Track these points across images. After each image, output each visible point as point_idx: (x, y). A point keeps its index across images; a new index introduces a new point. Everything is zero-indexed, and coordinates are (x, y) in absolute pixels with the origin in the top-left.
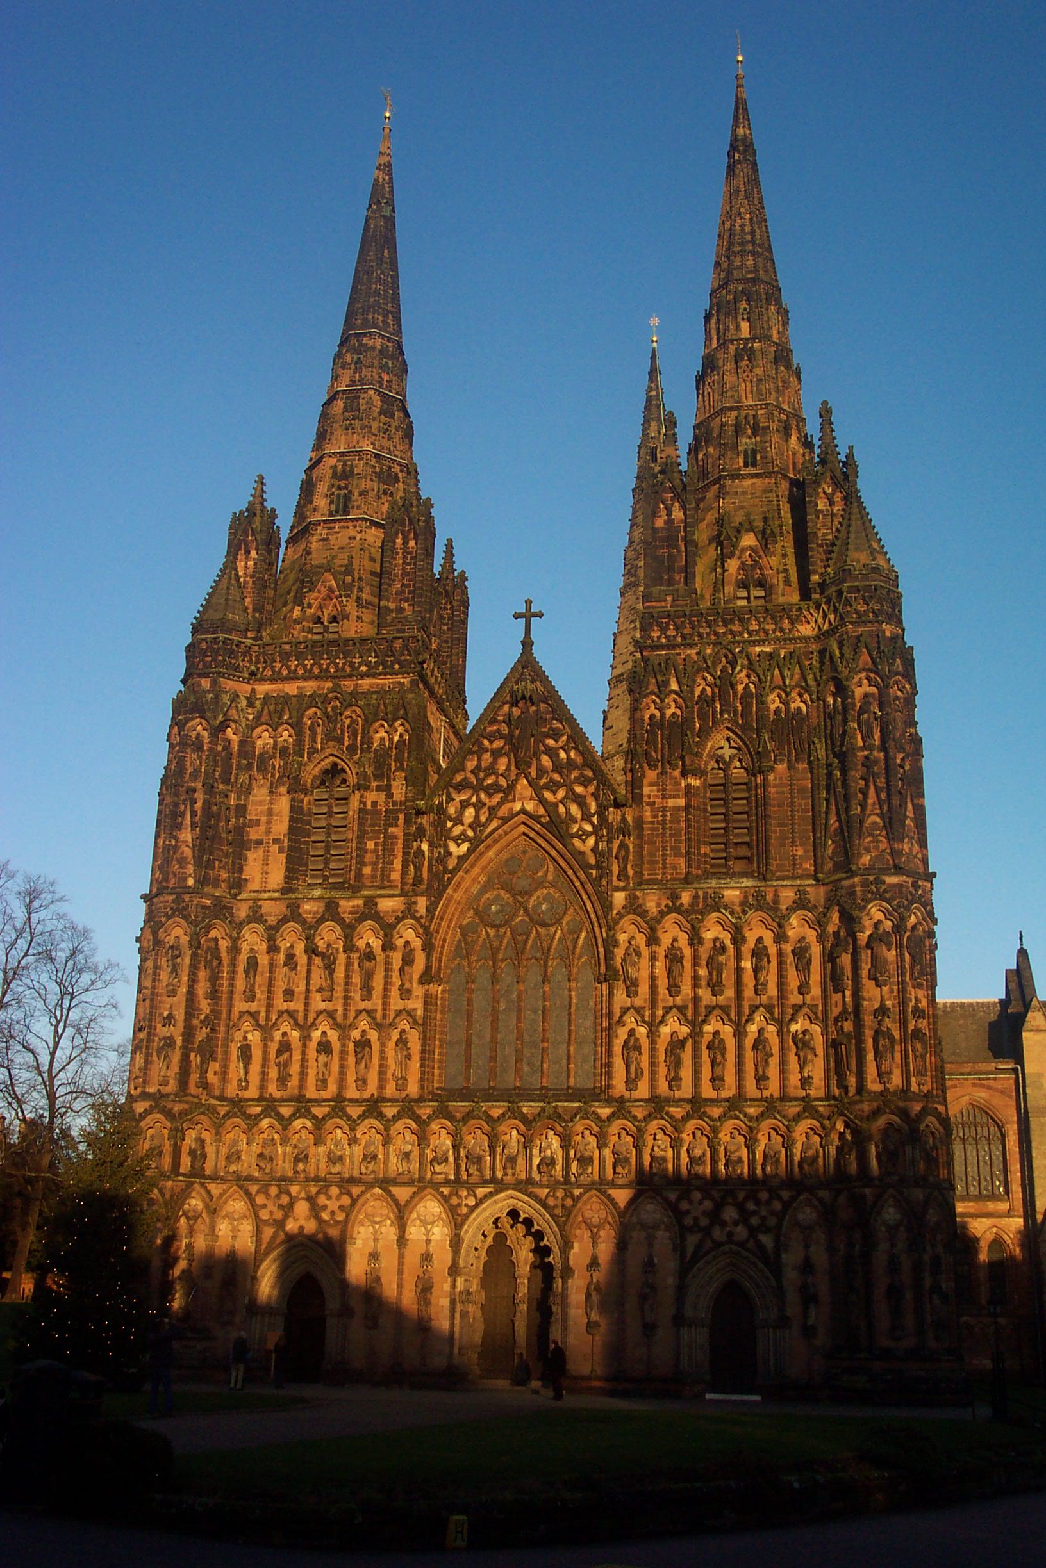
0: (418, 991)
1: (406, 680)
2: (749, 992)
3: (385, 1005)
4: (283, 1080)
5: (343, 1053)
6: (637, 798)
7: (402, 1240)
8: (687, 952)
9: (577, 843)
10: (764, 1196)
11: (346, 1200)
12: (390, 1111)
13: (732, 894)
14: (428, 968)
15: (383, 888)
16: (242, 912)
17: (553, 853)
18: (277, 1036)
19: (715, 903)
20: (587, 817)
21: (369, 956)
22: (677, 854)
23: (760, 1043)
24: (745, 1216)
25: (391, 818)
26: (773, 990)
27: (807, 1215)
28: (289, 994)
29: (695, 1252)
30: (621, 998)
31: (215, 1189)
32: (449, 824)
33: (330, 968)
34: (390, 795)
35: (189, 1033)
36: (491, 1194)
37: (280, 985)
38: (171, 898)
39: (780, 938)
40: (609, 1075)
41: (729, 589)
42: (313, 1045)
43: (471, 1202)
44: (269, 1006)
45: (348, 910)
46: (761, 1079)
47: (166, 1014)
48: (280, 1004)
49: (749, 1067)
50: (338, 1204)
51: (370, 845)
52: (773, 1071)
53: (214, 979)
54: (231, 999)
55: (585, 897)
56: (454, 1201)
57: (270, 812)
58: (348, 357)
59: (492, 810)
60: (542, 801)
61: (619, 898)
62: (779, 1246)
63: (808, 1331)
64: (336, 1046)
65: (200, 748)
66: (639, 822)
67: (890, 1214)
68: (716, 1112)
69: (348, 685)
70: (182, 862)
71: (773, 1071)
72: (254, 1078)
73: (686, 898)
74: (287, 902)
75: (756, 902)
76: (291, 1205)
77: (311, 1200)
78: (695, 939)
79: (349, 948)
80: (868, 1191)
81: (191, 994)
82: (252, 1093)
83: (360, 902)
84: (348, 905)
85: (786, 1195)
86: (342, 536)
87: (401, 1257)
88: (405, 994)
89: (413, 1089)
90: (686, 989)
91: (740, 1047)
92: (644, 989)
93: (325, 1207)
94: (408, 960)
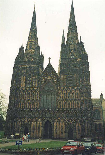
0: (39, 97)
1: (37, 65)
2: (72, 97)
3: (35, 99)
4: (25, 106)
5: (31, 103)
6: (60, 77)
7: (37, 123)
8: (66, 93)
9: (55, 82)
10: (74, 119)
11: (31, 119)
14: (40, 95)
15: (35, 86)
16: (20, 89)
18: (24, 102)
19: (69, 88)
20: (56, 79)
21: (34, 94)
23: (73, 103)
24: (72, 121)
25: (36, 79)
26: (74, 97)
27: (78, 121)
28: (25, 98)
30: (59, 98)
31: (17, 118)
33: (30, 95)
35: (15, 102)
36: (45, 119)
37: (24, 97)
39: (75, 92)
40: (58, 106)
41: (70, 56)
42: (28, 103)
43: (44, 119)
44: (23, 99)
46: (73, 107)
48: (24, 99)
49: (72, 105)
51: (34, 82)
52: (75, 106)
53: (17, 96)
54: (19, 98)
57: (23, 79)
58: (31, 31)
59: (46, 79)
60: (51, 78)
61: (59, 88)
62: (76, 124)
63: (79, 133)
64: (30, 103)
65: (16, 72)
66: (61, 80)
67: (87, 121)
68: (69, 110)
69: (31, 66)
70: (14, 84)
71: (75, 106)
72: (22, 107)
73: (65, 88)
75: (73, 88)
76: (25, 120)
77: (27, 119)
79: (32, 93)
80: (84, 118)
81: (15, 97)
82: (21, 108)
84: (31, 88)
85: (76, 119)
86: (30, 51)
87: (37, 125)
88: (37, 98)
89: (38, 107)
90: (66, 97)
91: (71, 103)
92: (61, 97)
93: (29, 120)
94: (38, 94)
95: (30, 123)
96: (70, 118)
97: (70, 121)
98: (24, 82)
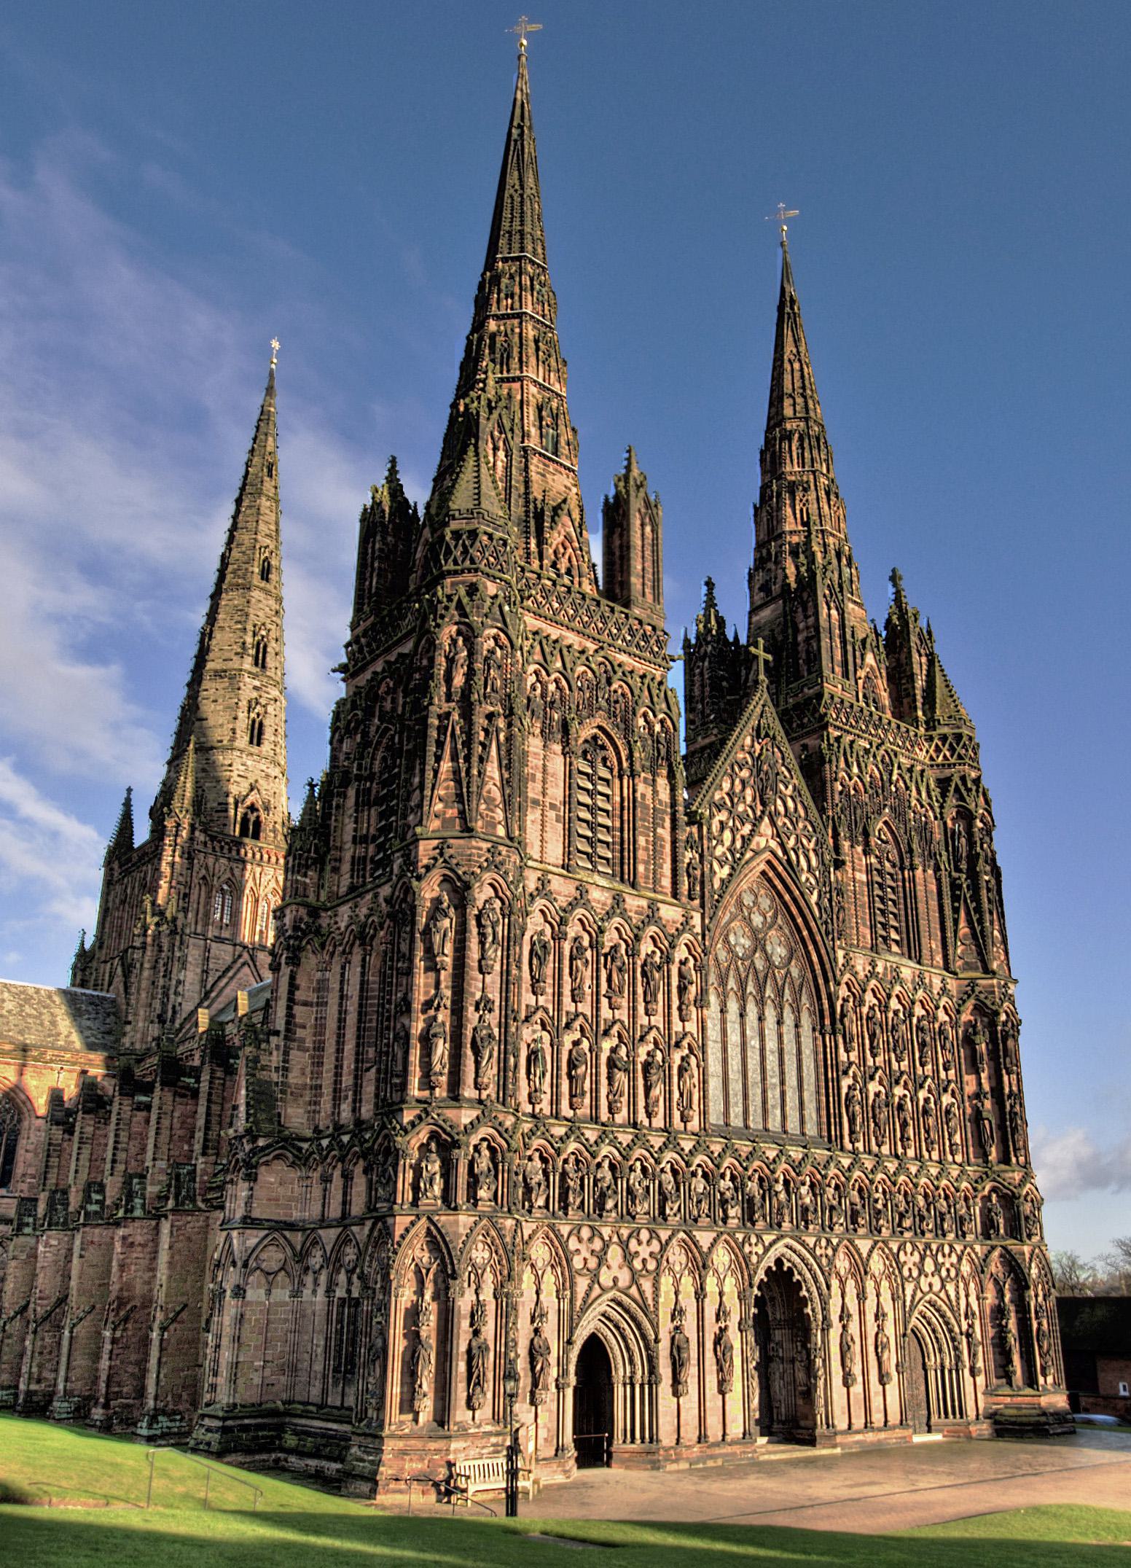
7: (700, 1294)
10: (947, 1249)
11: (655, 1246)
12: (687, 1145)
13: (906, 973)
17: (787, 897)
22: (864, 925)
24: (938, 1267)
29: (912, 1301)
32: (714, 842)
34: (655, 792)
36: (771, 1245)
38: (485, 845)
45: (634, 909)
47: (478, 995)
50: (649, 1249)
51: (641, 841)
55: (811, 947)
56: (747, 1249)
63: (973, 1372)
70: (489, 801)
73: (880, 969)
74: (577, 883)
75: (920, 982)
77: (624, 1245)
78: (885, 1008)
82: (545, 1106)
83: (644, 903)
88: (682, 1020)
95: (647, 1286)
96: (928, 1246)
97: (929, 1266)
98: (551, 814)
